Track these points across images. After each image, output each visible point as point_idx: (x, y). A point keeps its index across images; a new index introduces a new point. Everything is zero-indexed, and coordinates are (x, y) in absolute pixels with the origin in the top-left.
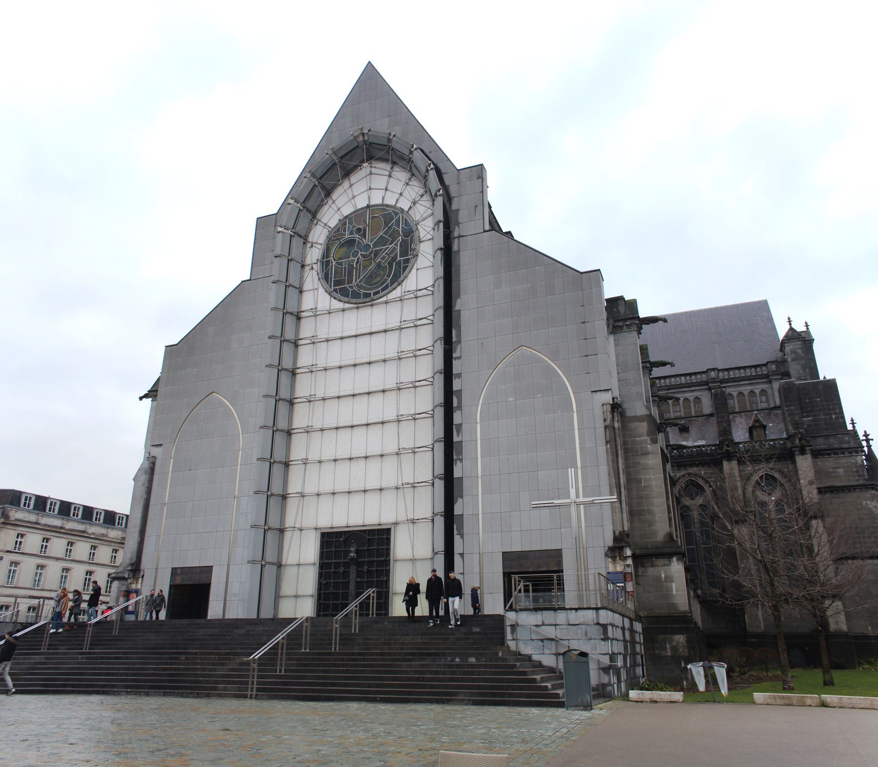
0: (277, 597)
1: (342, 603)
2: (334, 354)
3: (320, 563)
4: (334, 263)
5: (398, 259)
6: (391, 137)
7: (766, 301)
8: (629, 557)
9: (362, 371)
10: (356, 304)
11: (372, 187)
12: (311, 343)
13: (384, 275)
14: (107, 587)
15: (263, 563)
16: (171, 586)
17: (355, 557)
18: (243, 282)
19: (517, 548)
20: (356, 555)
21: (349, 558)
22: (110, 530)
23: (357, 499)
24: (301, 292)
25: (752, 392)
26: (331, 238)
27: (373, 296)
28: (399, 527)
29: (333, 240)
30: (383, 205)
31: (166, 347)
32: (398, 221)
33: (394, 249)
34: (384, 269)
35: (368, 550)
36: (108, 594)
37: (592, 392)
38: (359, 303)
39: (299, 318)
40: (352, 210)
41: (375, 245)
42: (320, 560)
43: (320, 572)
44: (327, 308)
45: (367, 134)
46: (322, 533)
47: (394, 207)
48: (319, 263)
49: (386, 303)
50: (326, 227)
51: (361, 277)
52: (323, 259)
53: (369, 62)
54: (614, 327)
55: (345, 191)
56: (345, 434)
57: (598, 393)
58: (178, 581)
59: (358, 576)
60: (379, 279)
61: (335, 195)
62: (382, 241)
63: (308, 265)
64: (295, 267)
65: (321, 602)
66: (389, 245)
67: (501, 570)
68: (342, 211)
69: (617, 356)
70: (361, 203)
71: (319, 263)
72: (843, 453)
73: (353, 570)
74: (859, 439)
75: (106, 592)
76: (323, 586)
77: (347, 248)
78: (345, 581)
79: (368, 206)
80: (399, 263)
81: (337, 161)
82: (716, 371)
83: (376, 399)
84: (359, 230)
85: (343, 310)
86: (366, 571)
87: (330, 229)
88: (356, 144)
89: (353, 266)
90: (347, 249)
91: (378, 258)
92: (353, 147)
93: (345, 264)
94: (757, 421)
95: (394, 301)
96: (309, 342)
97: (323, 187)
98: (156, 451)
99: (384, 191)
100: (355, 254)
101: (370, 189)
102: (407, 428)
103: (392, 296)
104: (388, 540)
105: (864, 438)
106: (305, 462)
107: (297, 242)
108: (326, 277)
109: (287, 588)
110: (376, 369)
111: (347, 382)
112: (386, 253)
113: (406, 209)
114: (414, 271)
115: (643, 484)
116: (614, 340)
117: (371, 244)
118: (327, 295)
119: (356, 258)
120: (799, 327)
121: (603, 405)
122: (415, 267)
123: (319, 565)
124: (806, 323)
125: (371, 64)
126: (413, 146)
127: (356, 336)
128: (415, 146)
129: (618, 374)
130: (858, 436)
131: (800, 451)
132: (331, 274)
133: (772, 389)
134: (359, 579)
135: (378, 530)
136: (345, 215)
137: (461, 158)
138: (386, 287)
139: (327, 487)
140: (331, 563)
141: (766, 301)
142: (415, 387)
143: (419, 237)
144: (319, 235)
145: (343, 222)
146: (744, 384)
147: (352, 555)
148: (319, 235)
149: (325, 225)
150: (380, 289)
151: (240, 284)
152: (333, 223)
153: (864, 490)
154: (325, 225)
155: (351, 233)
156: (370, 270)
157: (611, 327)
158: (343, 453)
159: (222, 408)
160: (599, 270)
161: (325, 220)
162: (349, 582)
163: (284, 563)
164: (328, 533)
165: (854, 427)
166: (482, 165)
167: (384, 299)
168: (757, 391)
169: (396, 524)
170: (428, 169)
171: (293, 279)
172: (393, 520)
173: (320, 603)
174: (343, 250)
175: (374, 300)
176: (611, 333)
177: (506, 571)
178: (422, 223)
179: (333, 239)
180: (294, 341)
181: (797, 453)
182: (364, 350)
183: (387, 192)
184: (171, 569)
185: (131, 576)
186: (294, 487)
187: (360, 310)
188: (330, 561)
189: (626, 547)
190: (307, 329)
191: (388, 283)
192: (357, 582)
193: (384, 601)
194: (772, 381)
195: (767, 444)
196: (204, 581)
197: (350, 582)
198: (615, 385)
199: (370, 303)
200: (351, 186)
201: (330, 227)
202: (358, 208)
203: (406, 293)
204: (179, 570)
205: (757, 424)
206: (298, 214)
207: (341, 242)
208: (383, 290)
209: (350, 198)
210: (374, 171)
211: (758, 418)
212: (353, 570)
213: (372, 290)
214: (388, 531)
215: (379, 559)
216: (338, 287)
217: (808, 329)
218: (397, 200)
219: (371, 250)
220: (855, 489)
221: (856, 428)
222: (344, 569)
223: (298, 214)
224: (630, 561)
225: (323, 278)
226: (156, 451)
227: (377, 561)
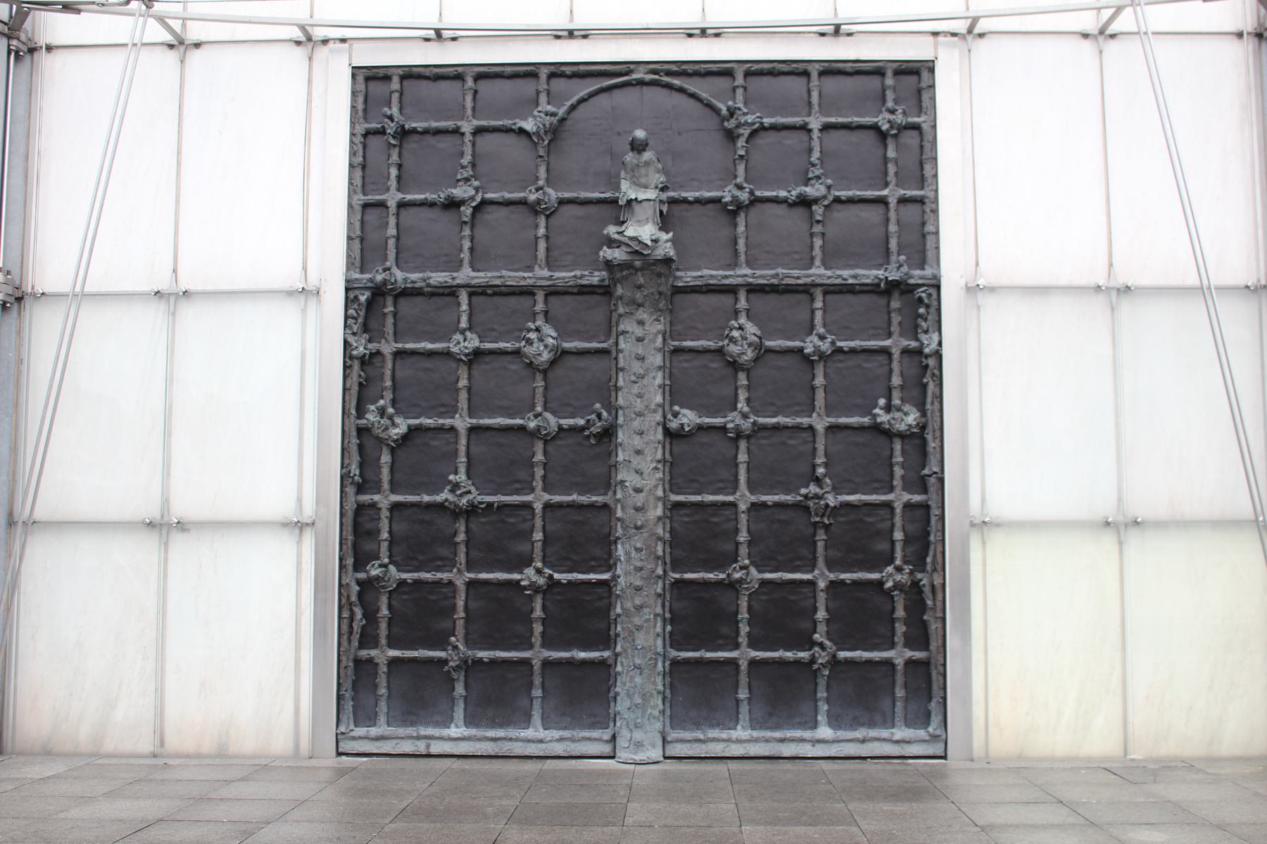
1: (553, 584)
35: (756, 201)
42: (350, 265)
59: (676, 393)
76: (386, 458)
78: (566, 422)
86: (750, 354)
123: (348, 302)
134: (688, 418)
147: (643, 230)
173: (367, 586)
188: (438, 278)
197: (621, 436)
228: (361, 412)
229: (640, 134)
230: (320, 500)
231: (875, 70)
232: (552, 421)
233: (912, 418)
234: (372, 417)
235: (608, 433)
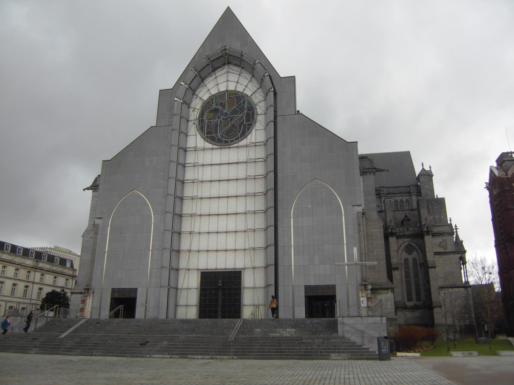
0: (176, 306)
2: (207, 174)
3: (200, 288)
4: (206, 121)
5: (245, 123)
6: (243, 53)
7: (409, 152)
8: (369, 289)
9: (224, 184)
10: (220, 146)
11: (229, 80)
12: (193, 166)
13: (236, 131)
14: (24, 294)
15: (169, 287)
16: (111, 298)
17: (222, 286)
18: (151, 127)
19: (312, 283)
20: (222, 284)
21: (218, 286)
22: (26, 260)
23: (221, 255)
24: (187, 136)
25: (402, 200)
27: (230, 142)
28: (246, 270)
29: (206, 108)
30: (235, 91)
31: (103, 161)
32: (244, 101)
33: (242, 117)
36: (24, 297)
37: (353, 205)
39: (185, 151)
41: (231, 113)
43: (201, 293)
44: (202, 147)
45: (229, 50)
46: (201, 272)
47: (242, 93)
48: (197, 120)
49: (238, 147)
50: (201, 99)
52: (200, 118)
53: (228, 7)
54: (363, 172)
55: (213, 80)
56: (214, 219)
57: (355, 206)
58: (116, 295)
60: (233, 133)
61: (206, 82)
62: (235, 112)
63: (191, 121)
64: (184, 121)
65: (201, 309)
66: (240, 114)
67: (304, 295)
69: (364, 187)
70: (222, 88)
71: (197, 120)
72: (445, 235)
73: (220, 292)
74: (453, 228)
75: (24, 296)
77: (214, 113)
79: (227, 91)
81: (209, 63)
82: (384, 188)
83: (233, 201)
85: (212, 149)
86: (228, 293)
87: (204, 101)
88: (221, 54)
89: (218, 124)
90: (214, 114)
91: (233, 121)
92: (220, 56)
93: (213, 123)
94: (406, 216)
96: (193, 165)
97: (201, 77)
98: (97, 221)
100: (219, 118)
101: (228, 81)
104: (240, 277)
105: (455, 228)
106: (191, 233)
107: (185, 107)
108: (201, 128)
109: (182, 301)
110: (232, 184)
111: (215, 190)
114: (254, 131)
115: (375, 253)
116: (363, 179)
118: (202, 139)
119: (220, 120)
121: (358, 213)
122: (254, 128)
123: (200, 289)
124: (430, 166)
125: (229, 8)
126: (256, 61)
127: (220, 164)
128: (257, 61)
129: (364, 196)
130: (452, 226)
131: (427, 234)
132: (205, 127)
133: (412, 199)
134: (223, 298)
135: (234, 272)
137: (283, 73)
138: (238, 138)
139: (204, 247)
140: (207, 288)
143: (257, 112)
145: (212, 98)
146: (398, 196)
147: (220, 284)
148: (197, 104)
149: (201, 98)
150: (234, 139)
151: (149, 129)
152: (206, 98)
153: (454, 254)
155: (217, 105)
156: (228, 127)
157: (361, 172)
158: (213, 229)
159: (141, 199)
160: (357, 142)
161: (200, 95)
162: (218, 298)
163: (180, 286)
164: (205, 272)
165: (451, 222)
166: (294, 76)
167: (236, 145)
168: (404, 200)
169: (244, 269)
170: (265, 75)
171: (183, 128)
173: (201, 310)
174: (212, 114)
176: (361, 175)
177: (307, 295)
178: (258, 104)
179: (205, 107)
180: (184, 164)
181: (425, 234)
182: (225, 172)
183: (238, 84)
184: (111, 289)
185: (86, 292)
186: (184, 246)
187: (222, 150)
189: (368, 284)
190: (191, 158)
191: (239, 136)
192: (222, 299)
193: (238, 309)
194: (412, 195)
195: (410, 229)
196: (132, 296)
198: (362, 202)
200: (216, 78)
201: (204, 100)
203: (251, 143)
204: (116, 290)
205: (406, 218)
206: (186, 90)
207: (209, 110)
208: (236, 140)
211: (407, 215)
212: (220, 292)
213: (229, 139)
214: (240, 272)
215: (235, 287)
216: (209, 135)
217: (430, 169)
218: (244, 90)
219: (228, 116)
220: (450, 254)
221: (452, 223)
222: (215, 291)
223: (186, 90)
224: (369, 292)
225: (199, 129)
226: (97, 221)
228: (201, 297)
229: (220, 277)
230: (198, 304)
231: (237, 272)
232: (214, 298)
233: (239, 297)
234: (202, 298)
235: (218, 299)
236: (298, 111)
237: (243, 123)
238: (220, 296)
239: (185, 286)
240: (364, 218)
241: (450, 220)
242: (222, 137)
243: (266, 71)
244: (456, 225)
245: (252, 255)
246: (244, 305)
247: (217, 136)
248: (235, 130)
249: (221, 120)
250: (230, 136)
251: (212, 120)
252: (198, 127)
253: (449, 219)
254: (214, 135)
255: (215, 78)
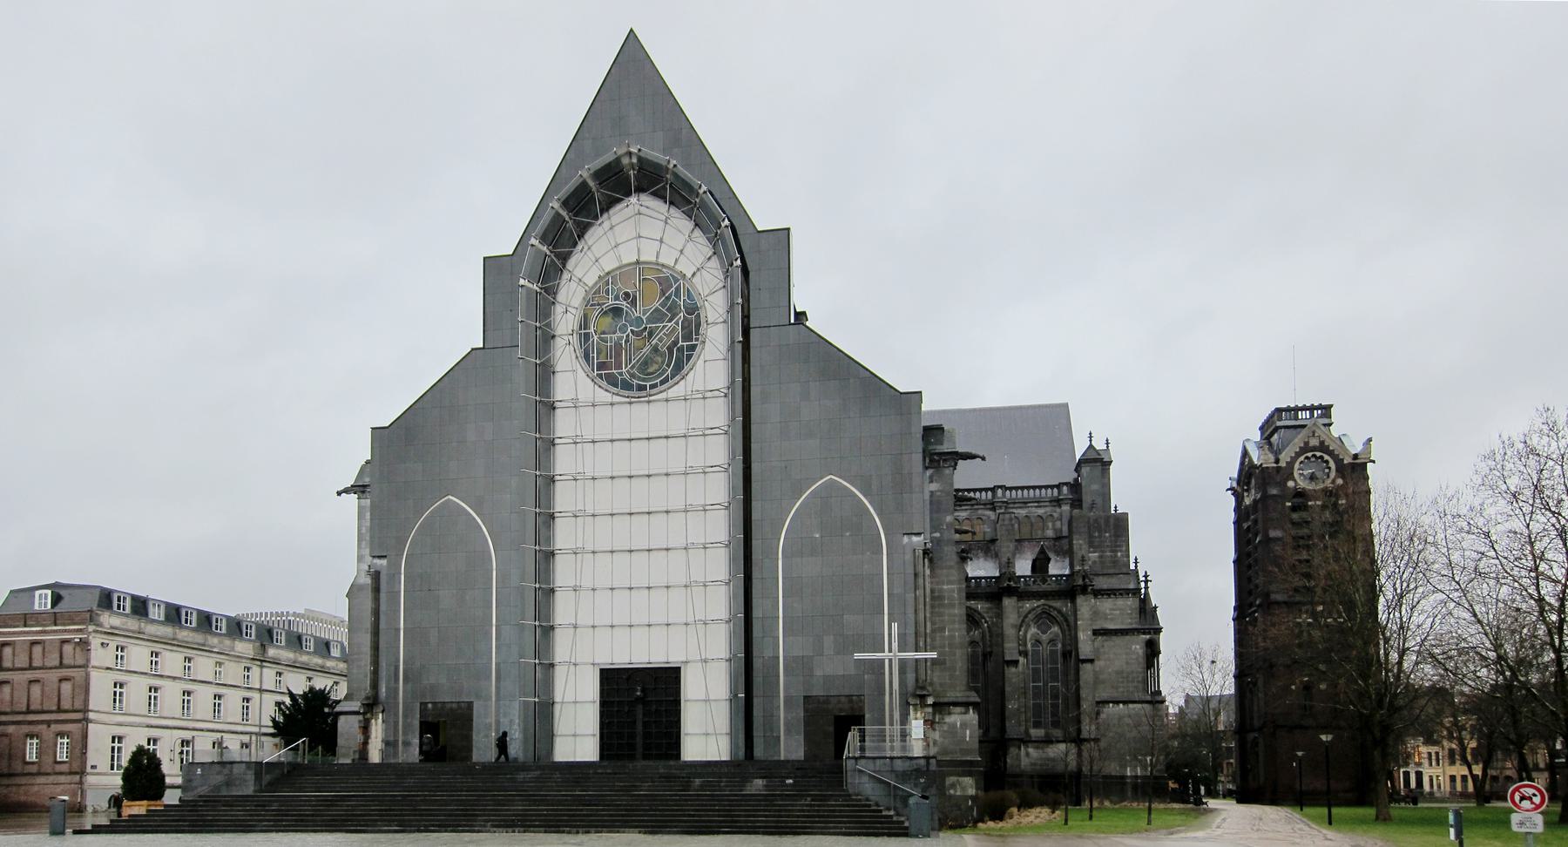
4: (595, 338)
5: (681, 343)
10: (628, 397)
13: (663, 362)
26: (589, 302)
29: (592, 305)
34: (662, 355)
38: (632, 397)
40: (616, 265)
41: (649, 320)
50: (581, 284)
51: (633, 362)
52: (580, 329)
59: (644, 715)
60: (655, 367)
66: (670, 321)
68: (602, 263)
73: (640, 709)
77: (613, 319)
80: (680, 350)
84: (627, 295)
87: (587, 288)
89: (621, 345)
95: (676, 399)
99: (658, 243)
101: (640, 237)
102: (696, 556)
103: (672, 393)
112: (665, 334)
113: (689, 275)
114: (700, 362)
117: (644, 318)
120: (1099, 445)
130: (1138, 576)
134: (647, 719)
136: (606, 271)
141: (1066, 406)
142: (705, 510)
144: (571, 295)
145: (607, 279)
147: (638, 693)
150: (658, 381)
152: (591, 279)
154: (580, 280)
155: (617, 298)
161: (578, 273)
165: (1136, 567)
167: (663, 396)
169: (686, 662)
172: (685, 659)
174: (608, 320)
175: (650, 396)
192: (644, 723)
199: (646, 399)
202: (625, 262)
208: (662, 383)
209: (613, 245)
210: (643, 210)
212: (640, 709)
215: (668, 699)
227: (666, 701)
236: (801, 316)
237: (675, 343)
238: (640, 716)
239: (569, 697)
240: (926, 560)
241: (1136, 563)
242: (632, 376)
243: (724, 213)
244: (1146, 572)
245: (701, 635)
246: (686, 734)
247: (621, 374)
248: (660, 359)
249: (628, 336)
250: (652, 373)
251: (609, 336)
252: (577, 351)
253: (1132, 560)
254: (615, 372)
255: (611, 229)
